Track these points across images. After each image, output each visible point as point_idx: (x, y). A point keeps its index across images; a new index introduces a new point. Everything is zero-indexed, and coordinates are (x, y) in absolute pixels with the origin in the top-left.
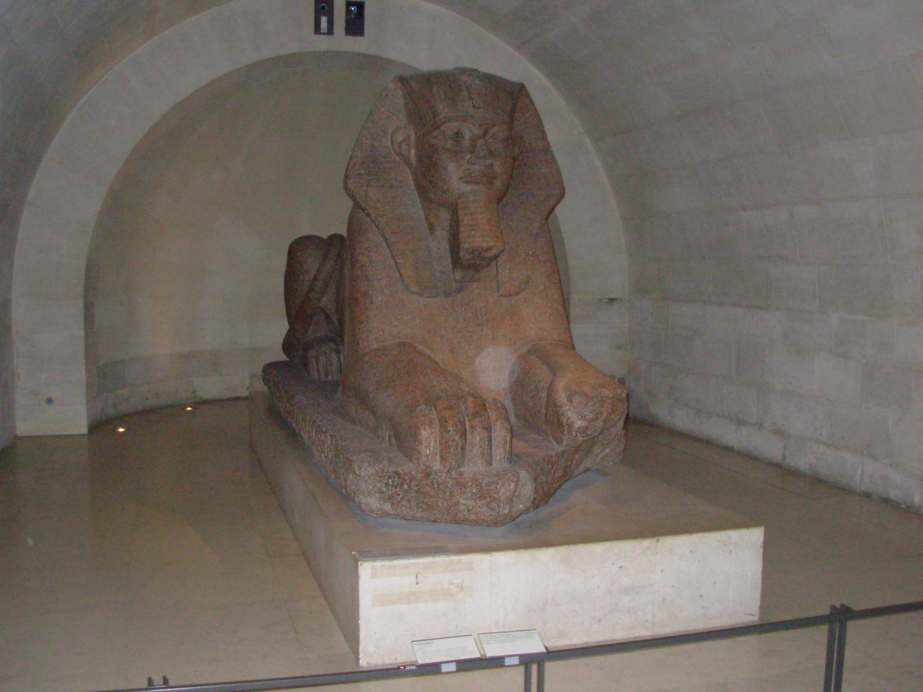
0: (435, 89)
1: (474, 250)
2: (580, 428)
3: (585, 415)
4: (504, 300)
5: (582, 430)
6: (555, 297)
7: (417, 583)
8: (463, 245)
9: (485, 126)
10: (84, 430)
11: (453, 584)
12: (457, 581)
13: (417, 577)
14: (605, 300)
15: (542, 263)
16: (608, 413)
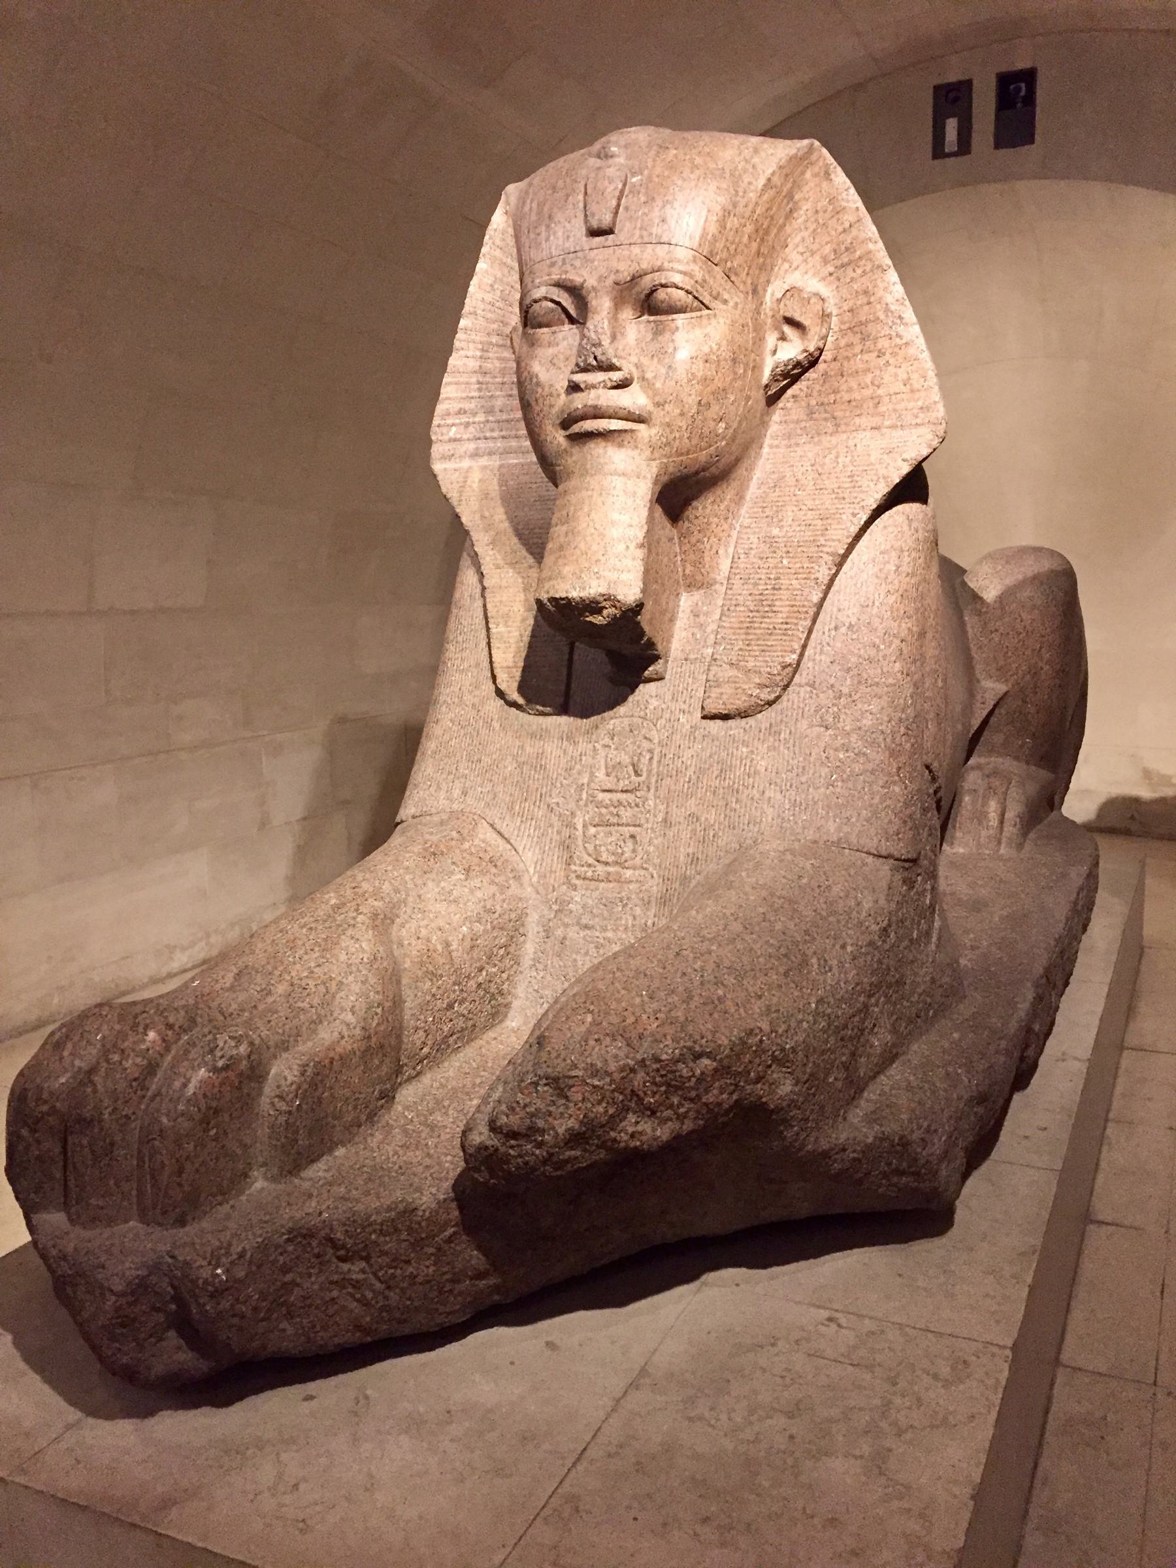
2: (482, 1148)
6: (867, 722)
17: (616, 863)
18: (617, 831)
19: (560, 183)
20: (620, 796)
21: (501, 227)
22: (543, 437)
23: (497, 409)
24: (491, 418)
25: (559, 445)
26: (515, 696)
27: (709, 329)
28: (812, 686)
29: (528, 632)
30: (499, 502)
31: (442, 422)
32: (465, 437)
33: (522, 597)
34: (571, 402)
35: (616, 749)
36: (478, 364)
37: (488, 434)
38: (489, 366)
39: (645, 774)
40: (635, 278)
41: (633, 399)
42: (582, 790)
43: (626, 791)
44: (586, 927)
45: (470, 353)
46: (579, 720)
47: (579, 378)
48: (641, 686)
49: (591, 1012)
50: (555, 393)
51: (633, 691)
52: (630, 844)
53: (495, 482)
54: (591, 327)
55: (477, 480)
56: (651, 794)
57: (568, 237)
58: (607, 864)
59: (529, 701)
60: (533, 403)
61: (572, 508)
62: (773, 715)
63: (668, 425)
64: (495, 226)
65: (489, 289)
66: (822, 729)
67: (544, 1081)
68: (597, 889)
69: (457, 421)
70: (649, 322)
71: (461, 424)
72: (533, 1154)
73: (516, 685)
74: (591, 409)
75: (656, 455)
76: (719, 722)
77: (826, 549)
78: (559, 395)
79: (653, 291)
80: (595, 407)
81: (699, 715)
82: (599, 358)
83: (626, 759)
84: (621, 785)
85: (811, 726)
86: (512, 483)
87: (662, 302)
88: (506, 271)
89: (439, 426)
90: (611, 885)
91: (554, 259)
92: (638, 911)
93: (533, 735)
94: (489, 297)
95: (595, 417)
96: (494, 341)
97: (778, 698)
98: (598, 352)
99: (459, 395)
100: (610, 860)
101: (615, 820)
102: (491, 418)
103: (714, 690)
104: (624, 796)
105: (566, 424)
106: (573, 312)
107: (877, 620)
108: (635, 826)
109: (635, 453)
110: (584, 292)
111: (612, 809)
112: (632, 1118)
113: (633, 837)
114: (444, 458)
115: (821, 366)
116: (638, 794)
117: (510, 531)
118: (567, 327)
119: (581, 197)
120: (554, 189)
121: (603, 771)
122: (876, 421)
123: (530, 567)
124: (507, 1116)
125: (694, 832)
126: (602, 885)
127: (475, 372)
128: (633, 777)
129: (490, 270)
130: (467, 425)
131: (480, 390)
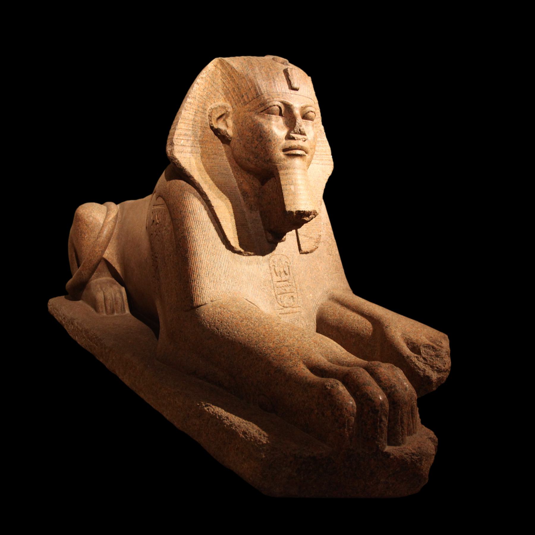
15: (325, 225)
17: (290, 306)
18: (286, 295)
19: (271, 67)
20: (283, 283)
21: (212, 70)
22: (274, 153)
23: (199, 136)
24: (197, 140)
25: (281, 155)
26: (239, 248)
28: (323, 242)
29: (234, 224)
30: (206, 173)
31: (179, 137)
32: (187, 145)
33: (228, 211)
34: (290, 143)
36: (193, 117)
37: (196, 145)
38: (197, 119)
39: (289, 274)
40: (306, 107)
41: (305, 145)
42: (271, 282)
43: (285, 281)
45: (191, 113)
46: (261, 257)
47: (293, 135)
48: (279, 244)
50: (282, 138)
51: (276, 245)
52: (291, 298)
53: (201, 164)
54: (299, 120)
55: (195, 163)
56: (293, 282)
58: (287, 307)
59: (245, 250)
60: (272, 141)
61: (293, 180)
62: (318, 251)
64: (210, 69)
65: (202, 90)
66: (329, 255)
69: (184, 138)
70: (304, 121)
71: (186, 139)
73: (238, 245)
74: (300, 147)
76: (305, 254)
77: (319, 199)
78: (283, 140)
79: (308, 112)
80: (302, 147)
81: (299, 253)
82: (302, 130)
83: (282, 270)
84: (283, 279)
85: (327, 255)
86: (208, 165)
87: (310, 116)
88: (210, 86)
89: (177, 139)
90: (291, 314)
91: (279, 93)
92: (303, 322)
93: (248, 264)
94: (201, 93)
95: (300, 150)
96: (200, 110)
98: (301, 128)
99: (185, 128)
100: (288, 306)
101: (284, 291)
102: (196, 139)
103: (303, 244)
104: (284, 283)
105: (285, 150)
106: (283, 112)
108: (291, 293)
109: (305, 163)
110: (292, 107)
111: (282, 288)
113: (292, 297)
114: (179, 152)
116: (289, 281)
117: (214, 184)
118: (278, 116)
119: (283, 75)
121: (274, 273)
122: (318, 162)
123: (226, 199)
126: (288, 315)
127: (192, 120)
128: (285, 276)
129: (204, 84)
130: (188, 140)
131: (193, 127)
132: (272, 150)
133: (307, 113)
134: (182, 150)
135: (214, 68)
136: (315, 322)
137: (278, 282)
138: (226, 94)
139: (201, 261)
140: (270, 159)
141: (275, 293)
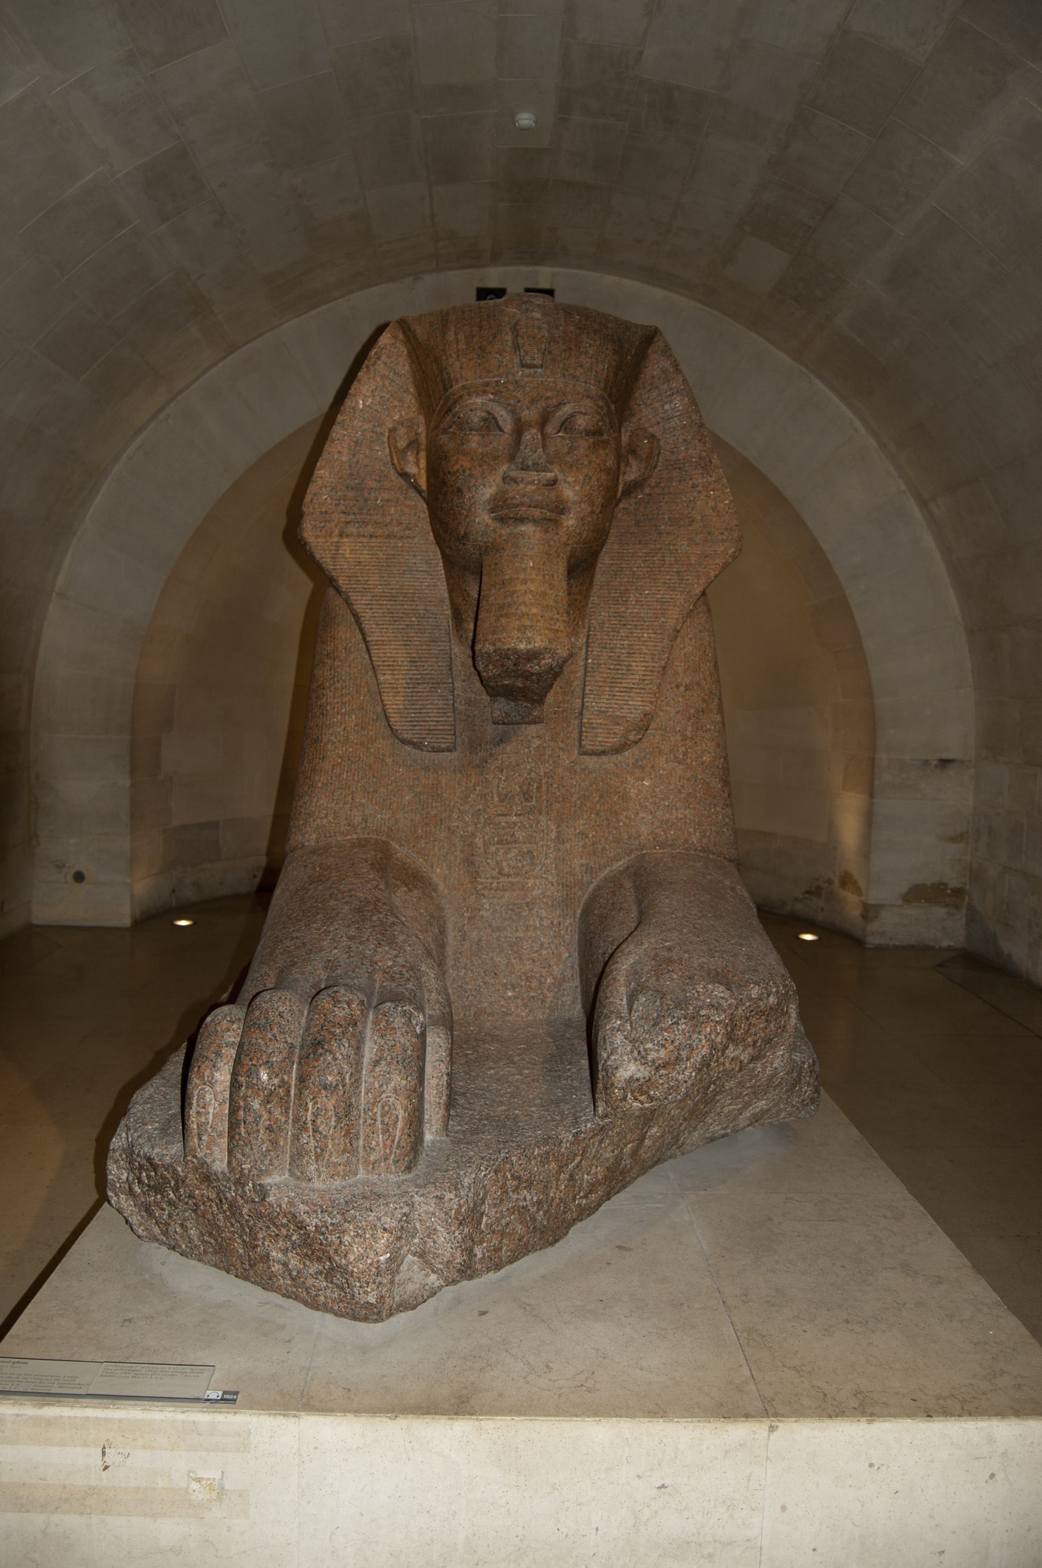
0: (451, 335)
1: (505, 655)
3: (645, 1050)
4: (590, 762)
5: (639, 1087)
6: (706, 758)
7: (106, 1468)
8: (480, 646)
9: (542, 404)
10: (127, 922)
11: (199, 1480)
12: (211, 1474)
13: (104, 1453)
14: (934, 763)
15: (682, 689)
16: (713, 1047)
19: (484, 323)
27: (607, 451)
35: (504, 781)
44: (498, 929)
47: (513, 474)
49: (673, 971)
57: (500, 366)
60: (465, 490)
63: (582, 519)
67: (683, 1021)
68: (503, 897)
72: (677, 1080)
75: (571, 542)
76: (595, 758)
88: (387, 383)
93: (426, 769)
97: (640, 739)
107: (703, 681)
112: (731, 1048)
115: (647, 490)
119: (509, 337)
120: (480, 327)
124: (658, 1051)
125: (584, 846)
126: (507, 894)
132: (465, 513)
133: (567, 419)
134: (323, 525)
135: (393, 341)
136: (577, 920)
137: (499, 815)
138: (420, 394)
139: (323, 758)
140: (466, 533)
141: (484, 840)
